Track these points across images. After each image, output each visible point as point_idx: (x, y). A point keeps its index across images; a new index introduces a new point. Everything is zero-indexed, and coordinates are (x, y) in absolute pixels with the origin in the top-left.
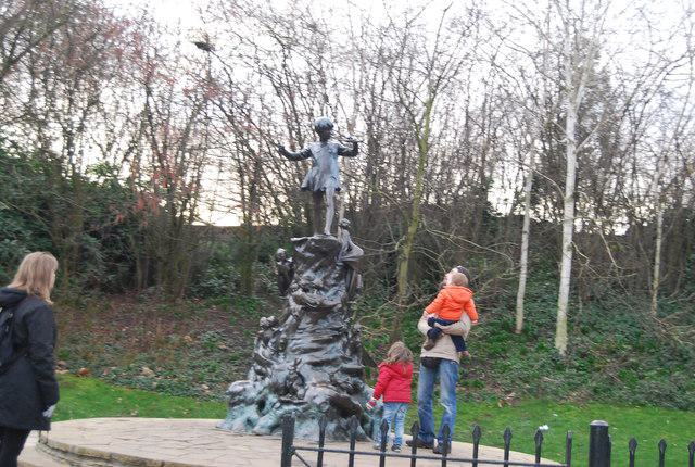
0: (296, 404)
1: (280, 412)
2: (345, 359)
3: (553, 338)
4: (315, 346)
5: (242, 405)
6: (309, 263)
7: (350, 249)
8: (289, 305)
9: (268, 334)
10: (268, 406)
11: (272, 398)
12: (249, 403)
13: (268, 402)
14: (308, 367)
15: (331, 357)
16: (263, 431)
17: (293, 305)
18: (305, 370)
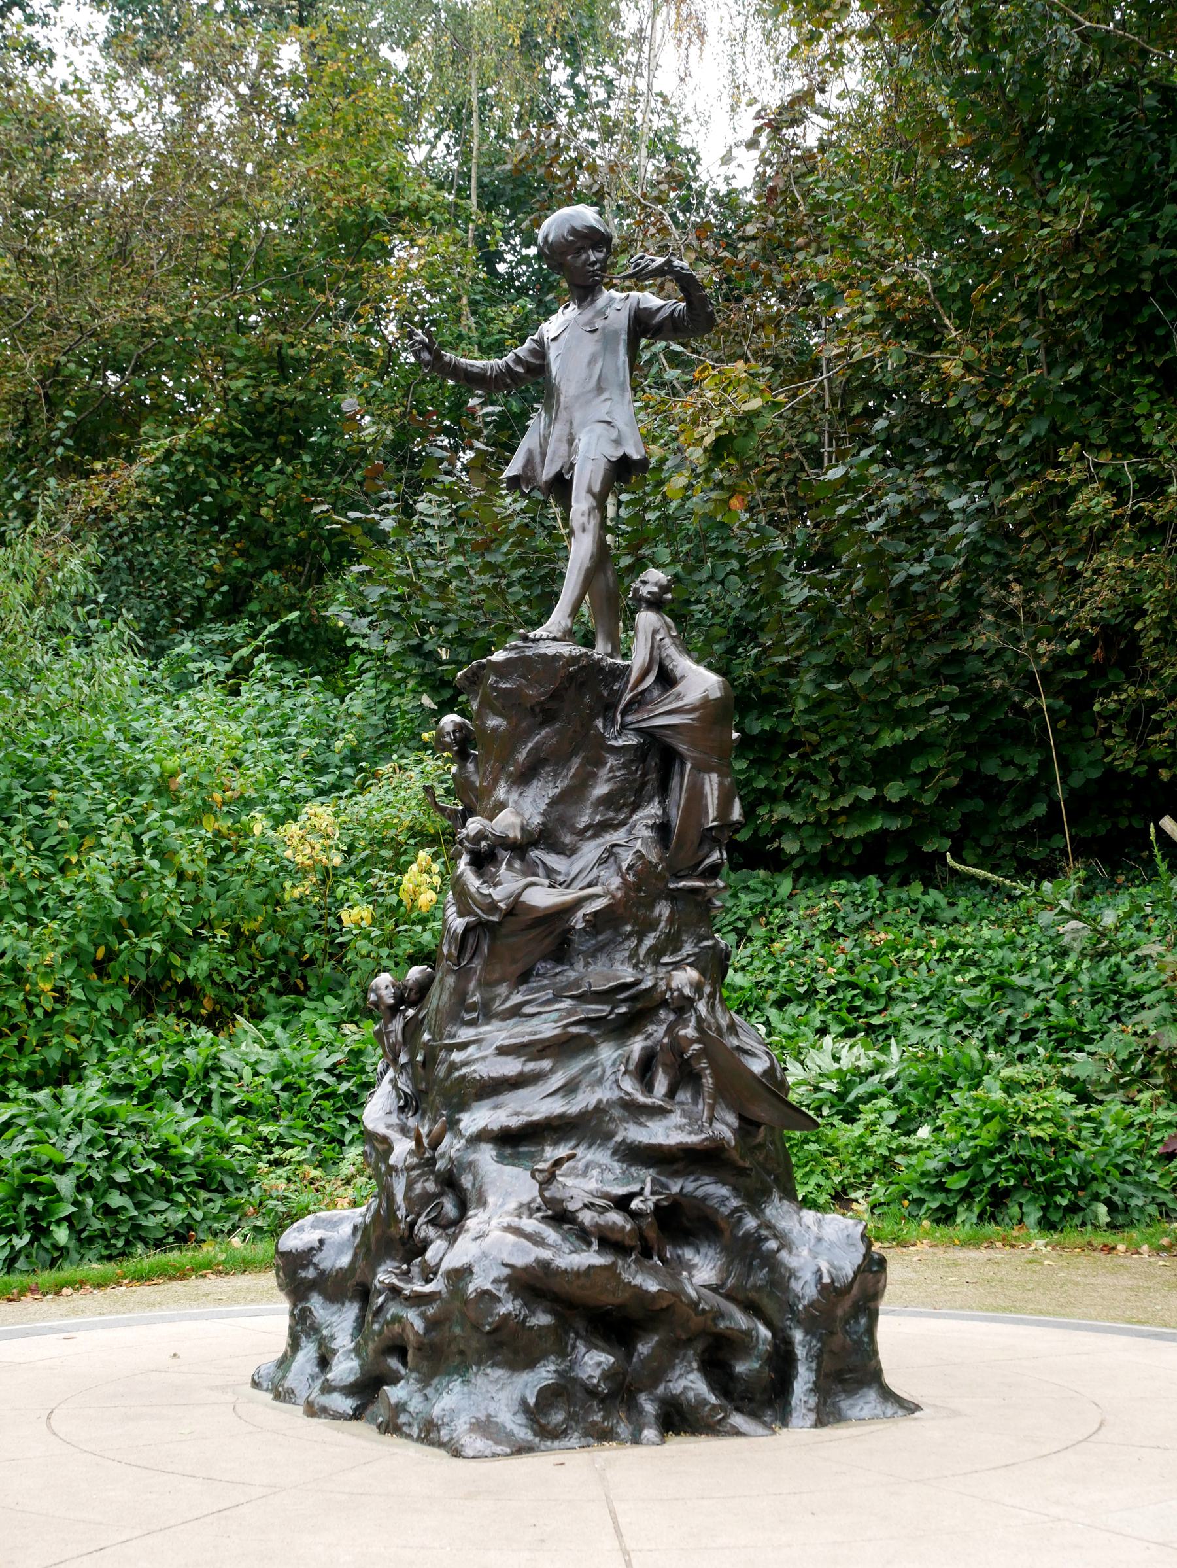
2: (635, 1111)
4: (511, 1067)
7: (667, 679)
14: (486, 1155)
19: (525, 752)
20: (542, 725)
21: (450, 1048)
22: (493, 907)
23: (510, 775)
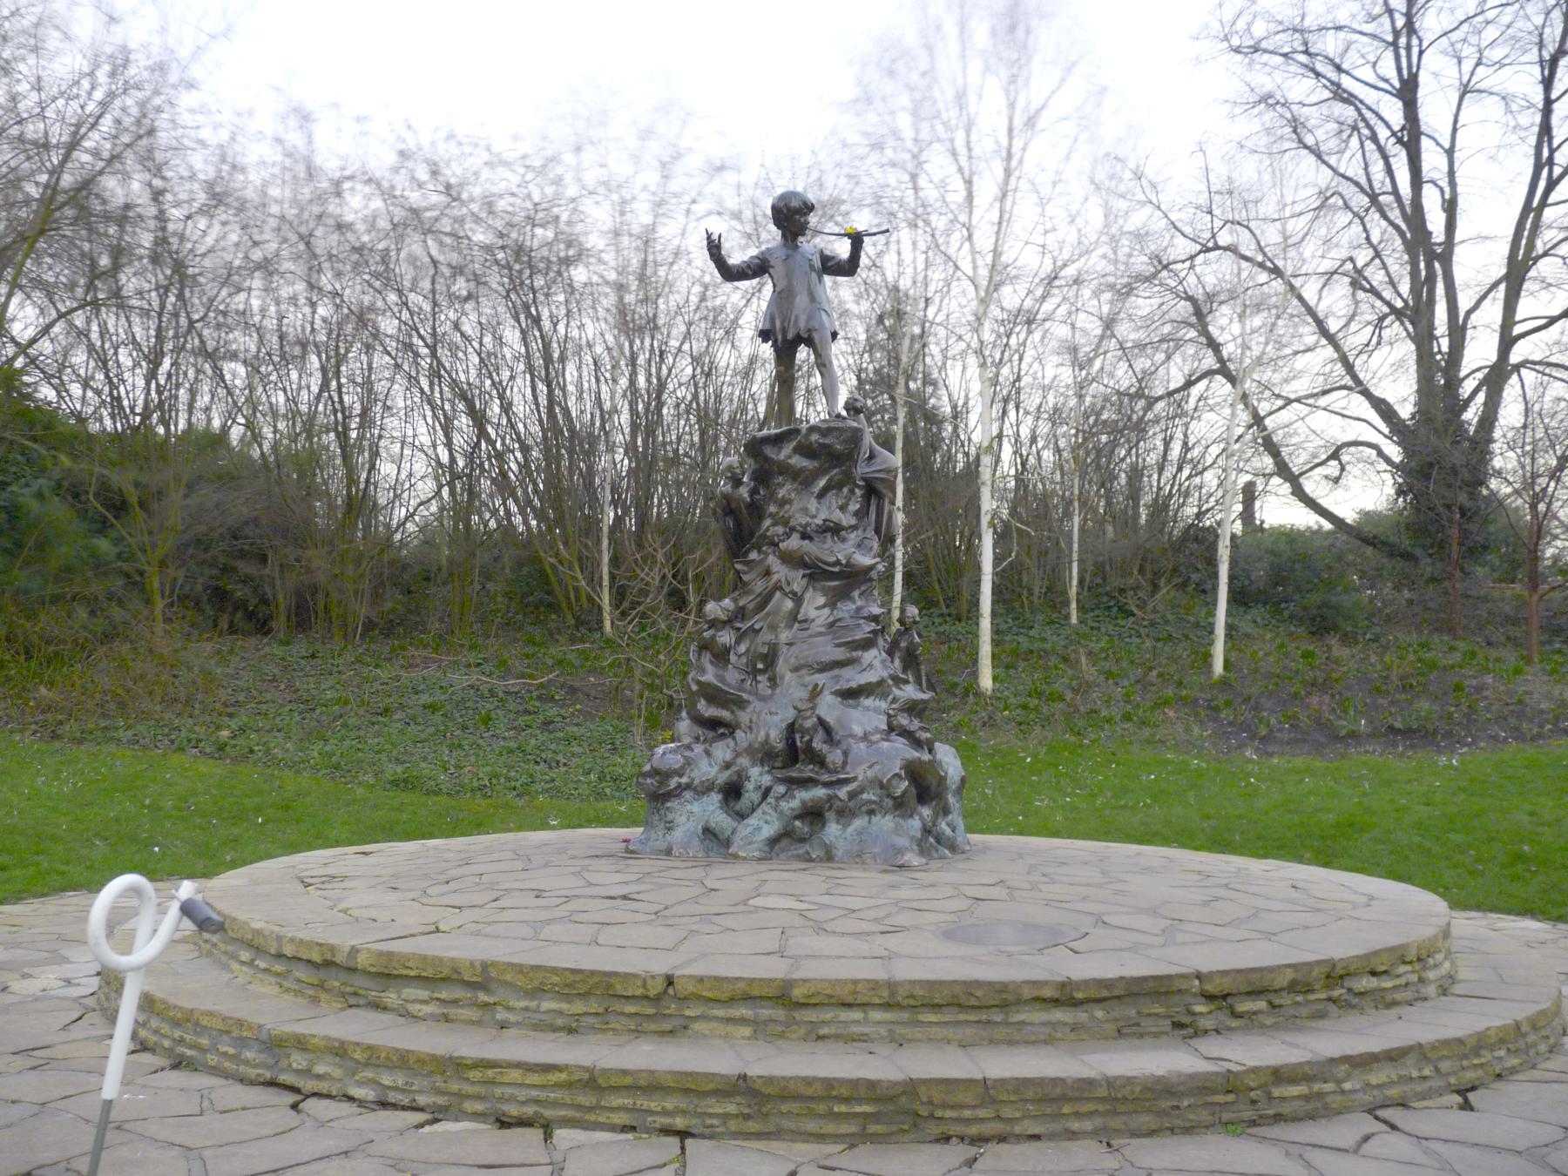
0: (826, 785)
2: (897, 681)
3: (975, 675)
4: (840, 654)
5: (688, 795)
6: (804, 480)
7: (872, 457)
8: (768, 573)
9: (725, 637)
10: (750, 795)
11: (758, 776)
12: (705, 789)
13: (750, 786)
15: (870, 677)
17: (780, 571)
18: (829, 708)
22: (838, 563)
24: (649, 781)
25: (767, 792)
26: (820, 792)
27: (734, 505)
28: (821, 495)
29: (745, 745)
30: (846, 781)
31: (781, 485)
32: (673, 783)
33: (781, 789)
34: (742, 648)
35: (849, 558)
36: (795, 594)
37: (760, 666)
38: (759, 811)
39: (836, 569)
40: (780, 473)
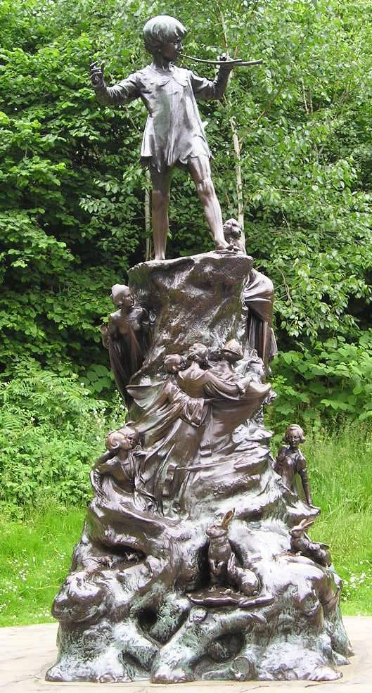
0: (245, 608)
1: (213, 625)
4: (239, 478)
5: (105, 623)
6: (197, 311)
8: (167, 401)
12: (120, 615)
16: (180, 673)
18: (237, 530)
19: (217, 310)
20: (225, 297)
21: (195, 471)
22: (239, 391)
23: (206, 322)
24: (66, 610)
25: (184, 615)
26: (238, 614)
27: (123, 331)
28: (211, 327)
29: (160, 570)
30: (259, 605)
31: (175, 315)
32: (92, 611)
33: (201, 613)
34: (146, 476)
35: (248, 387)
36: (197, 422)
37: (165, 492)
38: (179, 635)
39: (237, 399)
40: (173, 302)
